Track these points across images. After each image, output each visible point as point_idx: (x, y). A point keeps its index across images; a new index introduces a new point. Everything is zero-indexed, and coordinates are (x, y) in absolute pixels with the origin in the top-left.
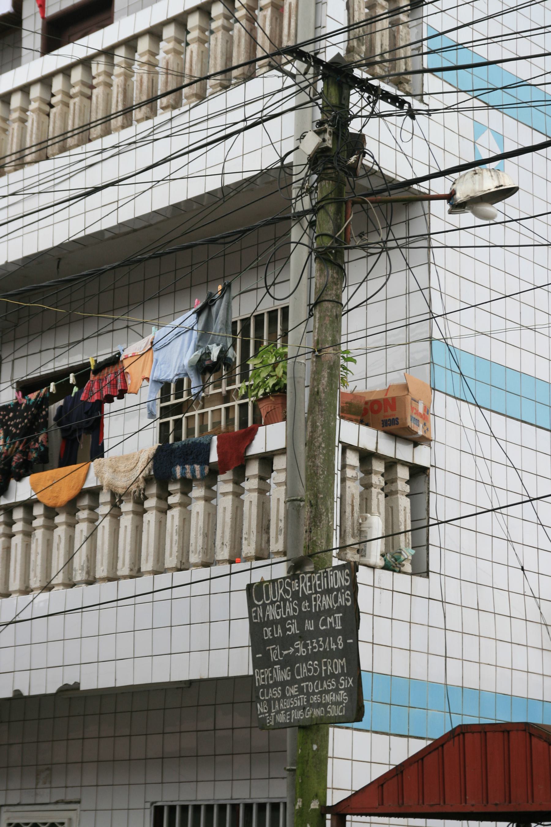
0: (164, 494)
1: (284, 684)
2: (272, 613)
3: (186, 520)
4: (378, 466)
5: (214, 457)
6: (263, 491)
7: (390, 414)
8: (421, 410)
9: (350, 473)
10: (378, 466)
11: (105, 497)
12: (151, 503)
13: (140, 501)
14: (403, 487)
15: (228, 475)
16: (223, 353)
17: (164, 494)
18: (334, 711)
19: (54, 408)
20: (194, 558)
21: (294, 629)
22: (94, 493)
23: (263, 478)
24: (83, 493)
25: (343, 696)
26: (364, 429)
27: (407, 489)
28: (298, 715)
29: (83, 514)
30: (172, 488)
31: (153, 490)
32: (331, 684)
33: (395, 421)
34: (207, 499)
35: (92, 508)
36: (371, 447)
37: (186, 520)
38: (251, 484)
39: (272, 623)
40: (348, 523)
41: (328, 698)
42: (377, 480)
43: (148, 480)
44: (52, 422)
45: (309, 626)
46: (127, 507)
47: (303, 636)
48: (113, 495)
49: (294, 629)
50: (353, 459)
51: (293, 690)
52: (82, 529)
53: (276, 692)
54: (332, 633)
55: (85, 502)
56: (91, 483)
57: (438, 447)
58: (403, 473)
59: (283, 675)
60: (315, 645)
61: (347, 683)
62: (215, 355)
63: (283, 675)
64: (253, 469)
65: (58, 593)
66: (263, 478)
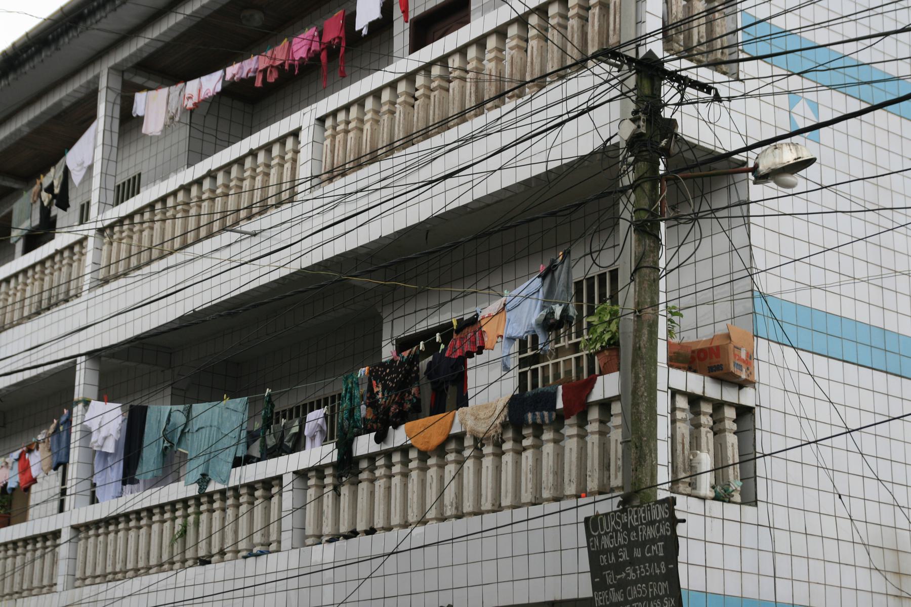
0: (518, 439)
3: (538, 461)
4: (707, 408)
5: (560, 405)
6: (603, 433)
7: (715, 361)
8: (743, 355)
9: (679, 415)
10: (707, 408)
11: (468, 442)
12: (508, 446)
13: (498, 444)
14: (730, 425)
15: (572, 420)
17: (518, 439)
20: (546, 494)
22: (459, 438)
23: (604, 421)
24: (450, 438)
26: (692, 376)
27: (734, 427)
29: (451, 457)
31: (509, 434)
33: (719, 367)
34: (556, 441)
35: (459, 451)
36: (699, 391)
37: (538, 461)
38: (593, 427)
40: (680, 460)
42: (706, 420)
43: (504, 426)
46: (488, 450)
48: (476, 439)
50: (682, 402)
52: (451, 469)
55: (452, 446)
56: (456, 430)
57: (762, 389)
58: (730, 413)
64: (594, 414)
65: (432, 526)
66: (604, 421)
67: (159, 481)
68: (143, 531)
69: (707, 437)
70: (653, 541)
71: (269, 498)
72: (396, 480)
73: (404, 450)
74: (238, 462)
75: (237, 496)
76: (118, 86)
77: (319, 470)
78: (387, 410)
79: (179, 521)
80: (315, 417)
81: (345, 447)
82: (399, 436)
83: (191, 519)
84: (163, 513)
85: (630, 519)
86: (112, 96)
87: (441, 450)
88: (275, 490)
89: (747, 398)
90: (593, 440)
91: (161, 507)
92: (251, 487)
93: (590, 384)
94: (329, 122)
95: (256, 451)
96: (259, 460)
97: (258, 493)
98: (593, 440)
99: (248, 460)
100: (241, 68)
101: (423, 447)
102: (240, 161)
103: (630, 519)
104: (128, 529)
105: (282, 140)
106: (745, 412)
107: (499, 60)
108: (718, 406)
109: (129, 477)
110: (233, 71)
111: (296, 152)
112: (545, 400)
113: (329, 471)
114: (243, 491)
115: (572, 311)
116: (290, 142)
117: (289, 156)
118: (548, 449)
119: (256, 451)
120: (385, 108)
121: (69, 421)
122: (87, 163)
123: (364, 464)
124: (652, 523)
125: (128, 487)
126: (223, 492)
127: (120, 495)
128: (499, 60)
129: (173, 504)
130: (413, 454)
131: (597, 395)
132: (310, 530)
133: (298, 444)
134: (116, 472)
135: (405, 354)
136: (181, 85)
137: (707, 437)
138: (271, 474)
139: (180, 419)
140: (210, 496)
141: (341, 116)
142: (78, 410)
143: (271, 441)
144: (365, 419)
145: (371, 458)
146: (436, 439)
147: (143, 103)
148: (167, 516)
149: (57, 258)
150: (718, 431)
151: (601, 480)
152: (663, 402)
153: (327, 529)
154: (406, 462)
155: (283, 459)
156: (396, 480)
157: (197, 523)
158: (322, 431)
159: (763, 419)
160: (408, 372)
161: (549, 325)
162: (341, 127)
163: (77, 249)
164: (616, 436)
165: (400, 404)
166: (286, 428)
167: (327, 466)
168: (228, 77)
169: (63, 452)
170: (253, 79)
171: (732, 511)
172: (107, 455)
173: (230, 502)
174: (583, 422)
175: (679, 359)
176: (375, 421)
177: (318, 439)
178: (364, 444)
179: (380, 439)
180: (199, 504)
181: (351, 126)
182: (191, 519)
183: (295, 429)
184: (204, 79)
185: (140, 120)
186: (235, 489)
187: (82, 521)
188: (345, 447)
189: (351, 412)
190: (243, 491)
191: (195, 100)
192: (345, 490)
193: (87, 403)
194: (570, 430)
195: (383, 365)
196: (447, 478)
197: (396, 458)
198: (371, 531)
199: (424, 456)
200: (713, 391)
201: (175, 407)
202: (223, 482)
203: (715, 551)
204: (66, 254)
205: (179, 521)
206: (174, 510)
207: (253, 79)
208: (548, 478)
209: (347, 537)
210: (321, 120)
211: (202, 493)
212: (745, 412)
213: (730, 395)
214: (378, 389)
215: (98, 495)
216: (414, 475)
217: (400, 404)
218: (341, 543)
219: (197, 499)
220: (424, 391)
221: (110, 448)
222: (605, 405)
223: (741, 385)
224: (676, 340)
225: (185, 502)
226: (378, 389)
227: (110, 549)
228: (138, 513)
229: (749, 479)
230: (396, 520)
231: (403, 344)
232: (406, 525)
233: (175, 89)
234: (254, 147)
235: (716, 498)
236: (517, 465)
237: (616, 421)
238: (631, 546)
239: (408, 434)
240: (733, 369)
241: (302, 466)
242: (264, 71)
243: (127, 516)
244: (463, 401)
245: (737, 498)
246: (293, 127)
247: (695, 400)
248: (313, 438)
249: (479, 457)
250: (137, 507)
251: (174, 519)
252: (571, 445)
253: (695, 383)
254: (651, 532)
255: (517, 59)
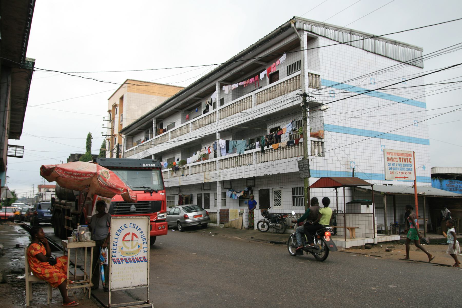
0: (289, 148)
1: (302, 173)
2: (301, 165)
3: (292, 151)
4: (317, 143)
5: (295, 143)
6: (301, 147)
7: (317, 136)
8: (322, 134)
9: (312, 144)
10: (317, 143)
11: (281, 148)
12: (287, 149)
13: (286, 148)
14: (320, 145)
15: (296, 145)
16: (295, 128)
17: (289, 148)
18: (307, 176)
19: (274, 135)
20: (293, 156)
21: (303, 167)
22: (280, 147)
23: (301, 145)
24: (279, 147)
25: (308, 175)
26: (314, 138)
27: (321, 145)
28: (304, 177)
29: (279, 150)
30: (290, 147)
31: (287, 147)
32: (307, 173)
33: (318, 136)
34: (294, 148)
35: (280, 149)
36: (315, 140)
37: (292, 151)
38: (300, 146)
39: (301, 166)
40: (312, 151)
41: (307, 175)
42: (316, 144)
43: (287, 146)
44: (274, 137)
45: (304, 166)
46: (284, 149)
47: (304, 167)
48: (283, 148)
49: (303, 167)
50: (313, 142)
51: (303, 174)
52: (279, 152)
53: (302, 174)
54: (307, 167)
55: (279, 148)
56: (279, 146)
58: (320, 143)
59: (302, 172)
60: (305, 168)
61: (309, 173)
62: (294, 128)
63: (302, 172)
64: (300, 144)
65: (277, 161)
66: (301, 145)
67: (232, 153)
68: (230, 161)
69: (317, 147)
70: (306, 165)
71: (251, 156)
72: (271, 153)
73: (272, 149)
74: (245, 150)
75: (246, 156)
76: (219, 84)
77: (259, 152)
78: (269, 143)
79: (236, 159)
80: (257, 143)
81: (263, 148)
82: (271, 147)
83: (238, 159)
84: (233, 158)
85: (303, 161)
86: (219, 86)
87: (277, 149)
88: (252, 155)
89: (323, 140)
90: (300, 148)
91: (233, 157)
92: (248, 154)
93: (299, 140)
94: (257, 94)
95: (248, 148)
96: (249, 150)
97: (249, 155)
98: (300, 148)
99: (247, 150)
100: (241, 83)
101: (275, 149)
102: (242, 100)
103: (303, 161)
104: (228, 161)
105: (249, 97)
106: (322, 143)
107: (284, 87)
108: (318, 142)
109: (227, 152)
110: (240, 84)
111: (252, 99)
112: (293, 142)
113: (260, 152)
114: (247, 155)
115: (296, 128)
116: (250, 97)
117: (250, 100)
118: (293, 149)
119: (248, 148)
120: (266, 93)
121: (216, 143)
122: (215, 98)
123: (266, 151)
124: (306, 162)
125: (227, 154)
126: (243, 155)
127: (226, 155)
128: (284, 87)
129: (235, 157)
130: (273, 150)
131: (300, 141)
132: (258, 161)
133: (255, 147)
134: (225, 151)
135: (271, 134)
136: (231, 85)
137: (317, 147)
138: (251, 152)
139: (235, 143)
140: (241, 155)
141: (259, 94)
142: (217, 141)
143: (250, 147)
144: (265, 144)
145: (267, 150)
146: (277, 147)
147: (224, 88)
148: (234, 158)
149: (211, 114)
150: (318, 146)
151: (301, 154)
152: (309, 143)
153: (260, 161)
154: (272, 151)
155: (253, 150)
156: (271, 153)
157: (239, 160)
158: (259, 145)
159: (325, 143)
160: (272, 137)
161: (292, 130)
162: (259, 95)
163: (215, 113)
164: (303, 147)
165: (271, 142)
166: (253, 145)
167: (260, 151)
168: (239, 85)
169: (215, 147)
170: (243, 85)
171: (320, 158)
172: (223, 148)
173: (245, 156)
174: (298, 145)
175: (312, 136)
176: (267, 144)
177: (258, 147)
178: (265, 148)
179: (268, 147)
180: (239, 157)
181: (261, 95)
182: (238, 159)
183: (254, 145)
184: (235, 85)
185: (224, 91)
186: (245, 154)
187: (220, 159)
188: (263, 148)
189: (263, 143)
190: (247, 155)
191: (234, 88)
192: (263, 156)
193: (219, 140)
194: (296, 146)
195: (268, 135)
196: (279, 154)
197: (271, 150)
198: (267, 161)
199: (275, 150)
200: (317, 140)
201: (234, 141)
202: (243, 153)
203: (318, 164)
204: (213, 114)
205: (236, 159)
206: (235, 158)
207: (243, 85)
208: (293, 154)
209: (264, 162)
210: (256, 94)
211: (240, 155)
212: (322, 143)
213: (320, 140)
214: (267, 139)
215: (222, 155)
216: (273, 153)
217: (271, 142)
218: (263, 163)
219: (239, 156)
220: (274, 140)
221: (223, 147)
222: (301, 143)
223: (322, 139)
224: (312, 132)
225: (237, 156)
226: (267, 139)
227: (225, 164)
228: (229, 158)
229: (323, 152)
230: (271, 160)
231: (271, 131)
232: (273, 160)
233: (230, 86)
234: (244, 98)
235: (318, 156)
236: (289, 151)
237: (303, 145)
238: (304, 165)
239: (272, 147)
240: (320, 137)
241: (256, 151)
242: (245, 84)
243: (227, 159)
244: (280, 141)
245: (321, 156)
246: (251, 95)
247: (315, 142)
248: (257, 146)
249: (283, 150)
250: (229, 157)
251: (235, 159)
252: (297, 149)
253: (315, 139)
254: (306, 163)
255: (286, 87)
